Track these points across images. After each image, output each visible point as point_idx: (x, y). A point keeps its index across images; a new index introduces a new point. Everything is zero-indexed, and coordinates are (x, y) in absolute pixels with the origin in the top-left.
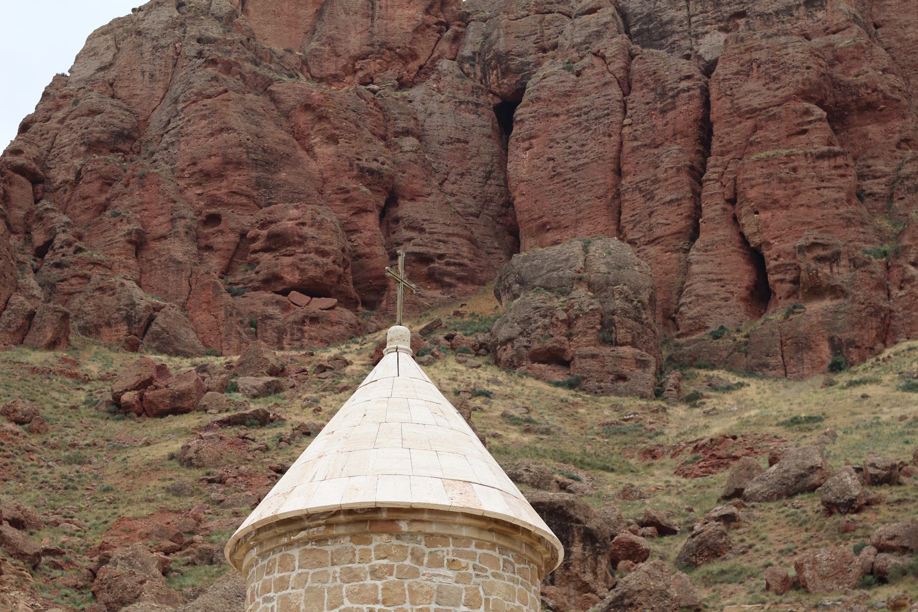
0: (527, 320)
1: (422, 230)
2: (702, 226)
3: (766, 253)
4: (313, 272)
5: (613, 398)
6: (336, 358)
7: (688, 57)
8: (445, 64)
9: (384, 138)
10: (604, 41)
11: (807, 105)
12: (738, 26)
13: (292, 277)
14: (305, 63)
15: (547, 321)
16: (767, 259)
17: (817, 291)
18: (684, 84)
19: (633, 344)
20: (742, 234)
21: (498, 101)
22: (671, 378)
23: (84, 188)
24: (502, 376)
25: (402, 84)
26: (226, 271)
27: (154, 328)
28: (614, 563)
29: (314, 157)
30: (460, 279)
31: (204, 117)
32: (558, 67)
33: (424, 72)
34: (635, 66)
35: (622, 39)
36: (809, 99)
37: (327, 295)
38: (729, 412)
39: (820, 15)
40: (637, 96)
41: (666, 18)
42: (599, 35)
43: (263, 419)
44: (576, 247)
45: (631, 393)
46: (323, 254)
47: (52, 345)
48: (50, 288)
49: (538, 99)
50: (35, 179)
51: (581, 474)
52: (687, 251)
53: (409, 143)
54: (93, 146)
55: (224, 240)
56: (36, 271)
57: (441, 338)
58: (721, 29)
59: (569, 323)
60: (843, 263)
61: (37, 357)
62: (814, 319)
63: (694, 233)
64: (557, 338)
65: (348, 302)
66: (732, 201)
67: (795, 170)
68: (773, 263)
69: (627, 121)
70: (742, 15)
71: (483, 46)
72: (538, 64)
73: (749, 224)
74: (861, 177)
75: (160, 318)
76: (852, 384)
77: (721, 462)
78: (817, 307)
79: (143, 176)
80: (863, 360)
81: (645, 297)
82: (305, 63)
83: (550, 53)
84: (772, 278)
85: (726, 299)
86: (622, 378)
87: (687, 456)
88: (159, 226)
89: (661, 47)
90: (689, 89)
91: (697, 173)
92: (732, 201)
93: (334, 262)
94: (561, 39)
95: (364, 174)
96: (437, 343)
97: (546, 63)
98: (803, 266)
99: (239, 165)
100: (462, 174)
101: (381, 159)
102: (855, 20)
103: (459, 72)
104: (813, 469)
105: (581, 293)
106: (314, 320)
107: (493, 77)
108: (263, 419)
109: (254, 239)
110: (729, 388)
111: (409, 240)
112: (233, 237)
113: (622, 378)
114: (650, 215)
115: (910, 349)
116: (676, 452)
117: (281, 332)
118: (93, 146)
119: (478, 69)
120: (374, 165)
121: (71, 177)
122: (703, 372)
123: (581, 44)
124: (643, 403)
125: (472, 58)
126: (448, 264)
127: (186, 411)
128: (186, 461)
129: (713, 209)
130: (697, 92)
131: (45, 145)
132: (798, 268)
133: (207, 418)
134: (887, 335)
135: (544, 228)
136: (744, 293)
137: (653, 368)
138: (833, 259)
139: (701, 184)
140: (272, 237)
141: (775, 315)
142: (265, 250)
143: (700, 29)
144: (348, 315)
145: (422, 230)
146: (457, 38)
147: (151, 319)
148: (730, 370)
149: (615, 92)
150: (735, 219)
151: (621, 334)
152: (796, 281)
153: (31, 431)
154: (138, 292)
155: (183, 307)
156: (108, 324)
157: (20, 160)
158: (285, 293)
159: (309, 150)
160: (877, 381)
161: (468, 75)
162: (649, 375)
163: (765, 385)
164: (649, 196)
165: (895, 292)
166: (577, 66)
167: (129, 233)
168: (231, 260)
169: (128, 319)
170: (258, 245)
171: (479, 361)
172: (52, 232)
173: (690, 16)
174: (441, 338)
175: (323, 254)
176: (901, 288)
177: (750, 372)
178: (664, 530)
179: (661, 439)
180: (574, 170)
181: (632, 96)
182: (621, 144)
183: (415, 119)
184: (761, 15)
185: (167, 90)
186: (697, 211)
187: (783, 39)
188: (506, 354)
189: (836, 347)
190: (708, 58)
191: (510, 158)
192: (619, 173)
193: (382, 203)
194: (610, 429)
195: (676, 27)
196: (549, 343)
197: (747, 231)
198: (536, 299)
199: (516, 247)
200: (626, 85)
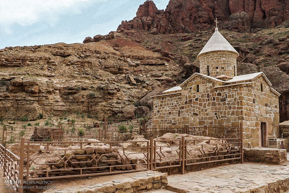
0: (232, 24)
1: (218, 13)
4: (204, 20)
9: (212, 2)
13: (202, 21)
17: (273, 15)
19: (247, 25)
20: (262, 9)
23: (175, 13)
26: (193, 22)
28: (245, 54)
29: (203, 6)
30: (224, 19)
31: (189, 2)
37: (207, 23)
43: (199, 40)
44: (239, 13)
46: (206, 18)
47: (173, 33)
48: (172, 26)
50: (169, 13)
51: (240, 43)
54: (176, 8)
55: (193, 18)
59: (238, 23)
61: (171, 35)
62: (272, 19)
63: (255, 9)
64: (237, 26)
65: (209, 24)
66: (260, 4)
75: (186, 28)
76: (278, 28)
79: (182, 11)
81: (248, 19)
84: (266, 14)
88: (185, 17)
92: (260, 4)
95: (210, 7)
96: (221, 28)
99: (194, 8)
104: (272, 40)
105: (239, 19)
106: (205, 26)
108: (199, 40)
109: (197, 17)
110: (260, 30)
112: (194, 17)
113: (246, 30)
117: (201, 28)
118: (176, 8)
127: (190, 40)
128: (190, 46)
129: (257, 6)
131: (170, 8)
133: (192, 40)
134: (283, 20)
135: (234, 11)
136: (262, 17)
137: (250, 28)
138: (275, 10)
140: (199, 16)
141: (266, 20)
142: (198, 18)
144: (209, 25)
145: (218, 13)
151: (245, 24)
152: (270, 14)
155: (189, 27)
156: (180, 30)
157: (167, 11)
158: (201, 23)
159: (203, 5)
160: (281, 27)
164: (248, 5)
165: (284, 14)
168: (194, 20)
169: (182, 29)
170: (197, 18)
172: (172, 19)
175: (206, 18)
177: (263, 28)
178: (251, 50)
186: (255, 6)
188: (230, 28)
189: (275, 23)
192: (244, 2)
193: (213, 10)
194: (244, 37)
196: (235, 26)
199: (230, 14)
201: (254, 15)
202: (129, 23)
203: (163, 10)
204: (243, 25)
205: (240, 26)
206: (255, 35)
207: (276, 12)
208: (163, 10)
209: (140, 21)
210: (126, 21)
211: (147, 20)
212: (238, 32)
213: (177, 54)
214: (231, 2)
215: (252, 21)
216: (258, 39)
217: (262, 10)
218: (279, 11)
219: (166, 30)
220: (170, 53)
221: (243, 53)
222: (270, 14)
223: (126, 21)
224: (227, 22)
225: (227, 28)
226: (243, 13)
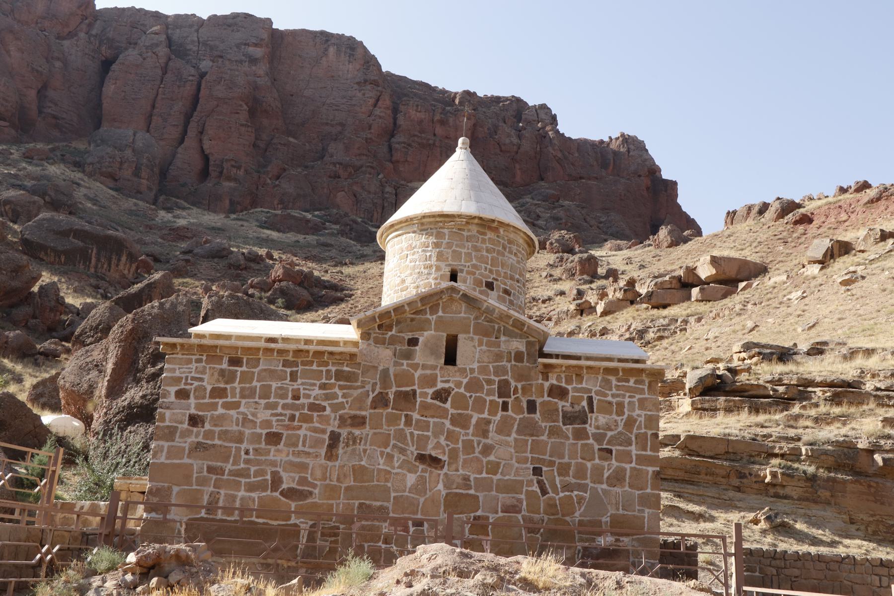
1: (56, 105)
2: (186, 139)
3: (211, 158)
5: (134, 200)
6: (6, 150)
7: (194, 67)
8: (82, 35)
9: (47, 59)
10: (159, 48)
11: (241, 103)
12: (218, 61)
14: (12, 11)
15: (111, 160)
16: (210, 160)
17: (229, 179)
18: (191, 78)
20: (202, 147)
21: (104, 59)
22: (162, 198)
24: (86, 178)
25: (59, 37)
29: (10, 56)
32: (136, 52)
33: (71, 35)
34: (171, 64)
35: (166, 50)
36: (243, 101)
37: (5, 120)
38: (184, 218)
39: (254, 68)
40: (169, 76)
41: (188, 47)
42: (157, 45)
44: (130, 132)
45: (142, 200)
49: (123, 64)
51: (119, 228)
52: (177, 148)
53: (58, 64)
57: (58, 154)
58: (211, 60)
60: (242, 170)
63: (182, 141)
66: (201, 133)
67: (230, 128)
68: (212, 163)
69: (162, 86)
70: (221, 57)
71: (102, 31)
72: (126, 49)
73: (206, 146)
74: (256, 139)
77: (182, 238)
78: (227, 184)
80: (242, 211)
81: (157, 162)
82: (12, 11)
83: (132, 46)
84: (210, 168)
85: (189, 172)
86: (139, 192)
87: (164, 232)
89: (183, 59)
90: (192, 81)
91: (188, 117)
93: (11, 106)
94: (139, 42)
96: (57, 156)
97: (130, 50)
98: (225, 167)
100: (80, 86)
101: (43, 67)
102: (267, 75)
103: (88, 40)
105: (128, 153)
107: (104, 48)
110: (184, 209)
111: (50, 107)
113: (141, 193)
114: (164, 128)
115: (262, 211)
116: (161, 229)
119: (97, 43)
120: (40, 69)
122: (174, 199)
123: (148, 46)
124: (148, 205)
125: (96, 36)
126: (66, 123)
129: (192, 132)
130: (196, 83)
132: (223, 168)
134: (254, 204)
137: (154, 192)
138: (239, 168)
139: (189, 123)
141: (209, 184)
143: (202, 57)
144: (13, 132)
145: (56, 105)
146: (90, 25)
148: (186, 201)
149: (160, 72)
150: (201, 140)
159: (8, 52)
160: (247, 221)
161: (92, 43)
162: (152, 195)
163: (199, 211)
166: (145, 55)
171: (76, 169)
173: (198, 50)
174: (58, 154)
175: (7, 101)
176: (263, 187)
177: (194, 204)
179: (154, 222)
180: (133, 99)
181: (167, 75)
182: (157, 95)
183: (63, 54)
184: (229, 60)
186: (185, 132)
187: (237, 73)
189: (232, 203)
190: (203, 70)
191: (105, 85)
192: (153, 107)
193: (40, 87)
194: (131, 213)
195: (191, 53)
196: (110, 170)
197: (205, 147)
198: (109, 150)
200: (165, 70)
201: (174, 155)
204: (137, 173)
205: (127, 173)
206: (168, 217)
207: (241, 173)
212: (116, 190)
214: (113, 87)
215: (163, 174)
216: (179, 234)
217: (203, 151)
218: (246, 170)
221: (131, 263)
222: (221, 172)
224: (81, 145)
225: (78, 165)
226: (142, 140)
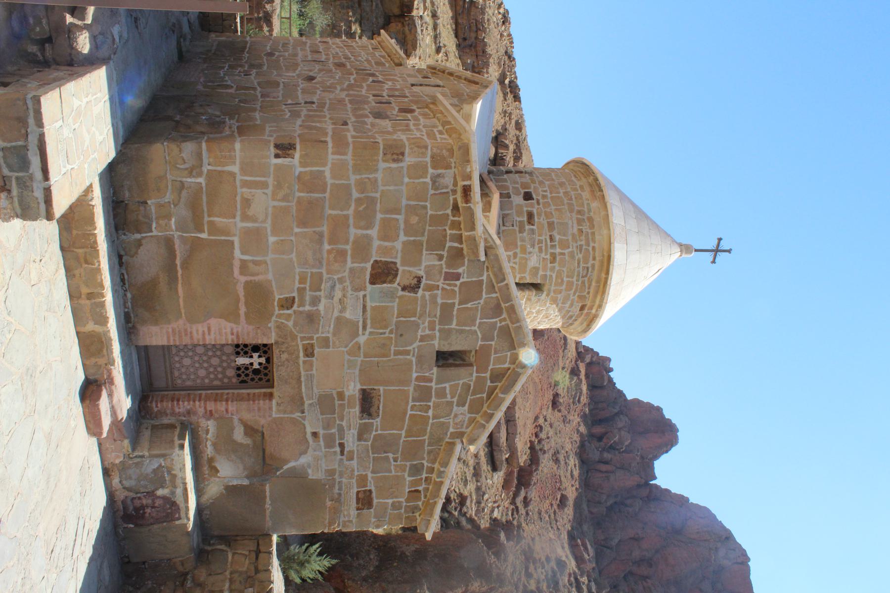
27: (605, 549)
56: (615, 503)
75: (609, 551)
121: (653, 510)
142: (644, 588)
147: (608, 548)
153: (558, 505)
154: (616, 541)
156: (603, 532)
167: (638, 534)
170: (645, 583)
185: (694, 539)
202: (606, 378)
203: (655, 478)
208: (655, 478)
209: (616, 411)
210: (611, 370)
211: (620, 429)
213: (529, 519)
219: (596, 491)
220: (533, 494)
223: (611, 370)
